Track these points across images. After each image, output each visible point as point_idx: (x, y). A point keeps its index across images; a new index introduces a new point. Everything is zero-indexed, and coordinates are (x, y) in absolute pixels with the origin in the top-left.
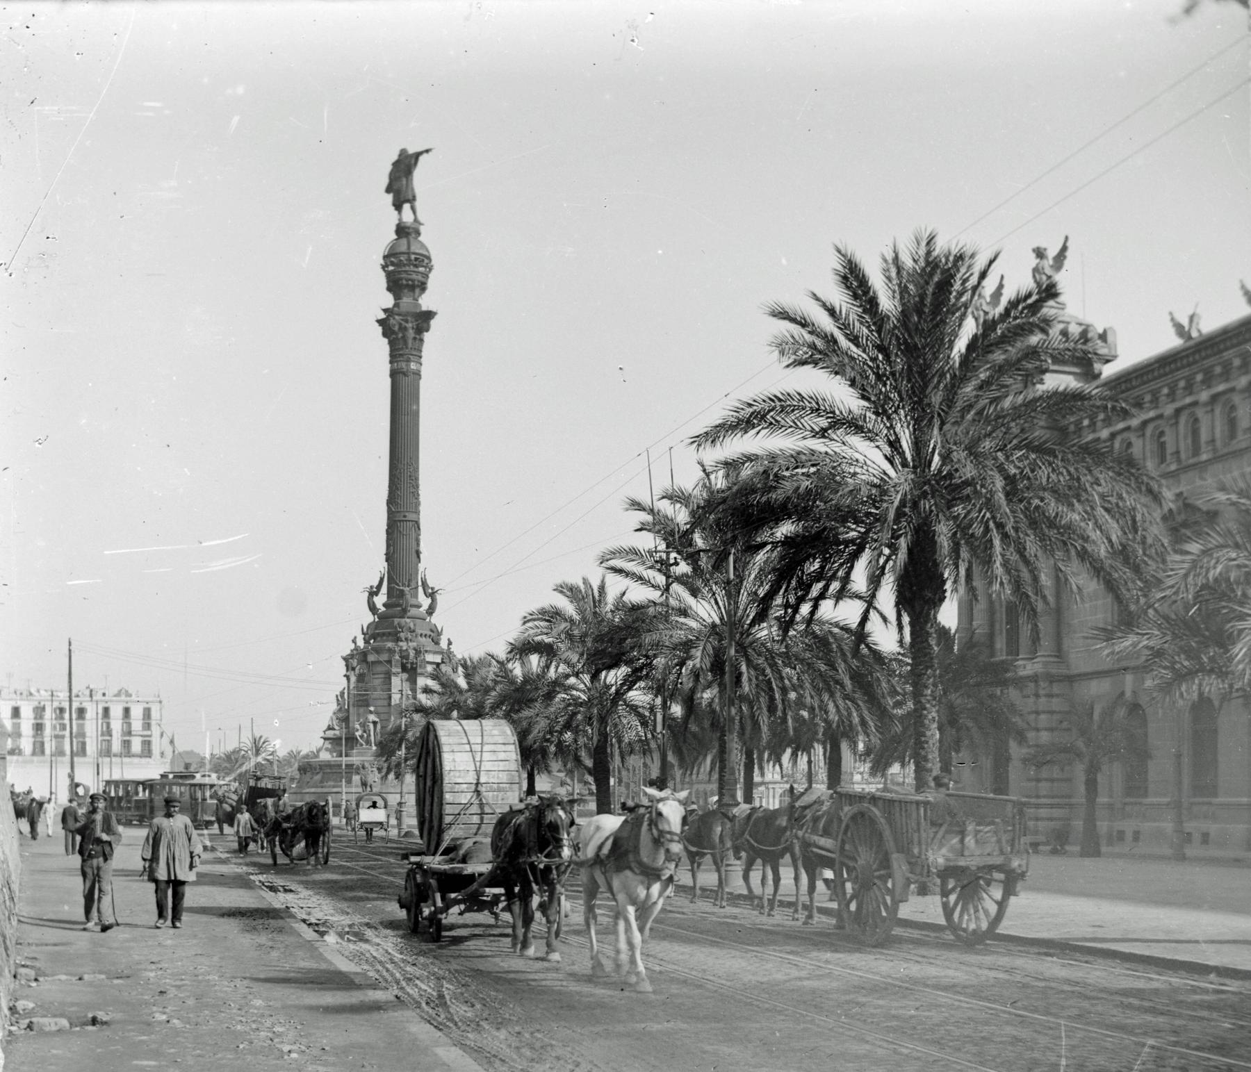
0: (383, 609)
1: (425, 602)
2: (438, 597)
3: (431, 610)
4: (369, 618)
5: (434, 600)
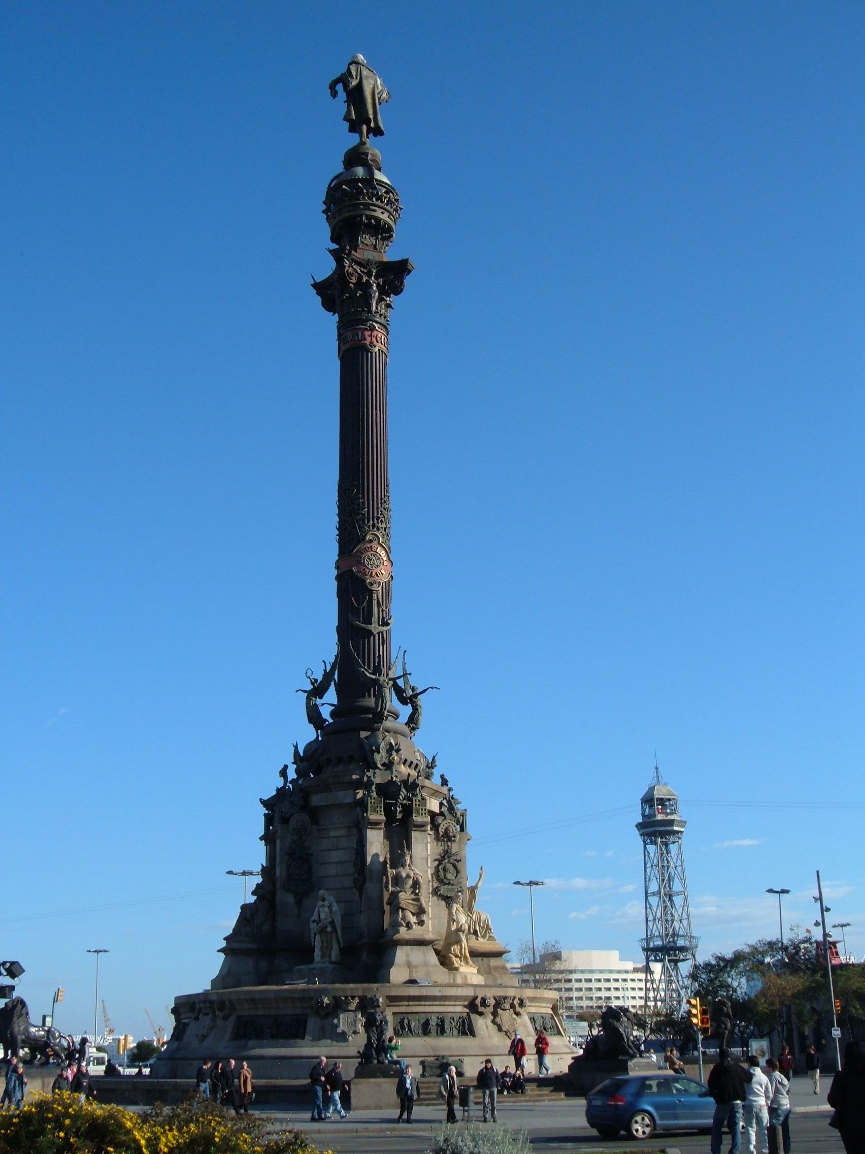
0: (331, 721)
1: (405, 711)
2: (422, 700)
3: (413, 722)
4: (308, 734)
5: (415, 709)
